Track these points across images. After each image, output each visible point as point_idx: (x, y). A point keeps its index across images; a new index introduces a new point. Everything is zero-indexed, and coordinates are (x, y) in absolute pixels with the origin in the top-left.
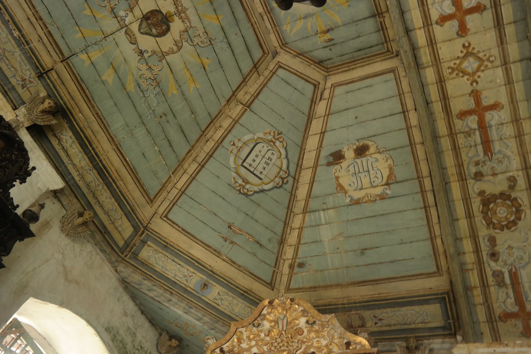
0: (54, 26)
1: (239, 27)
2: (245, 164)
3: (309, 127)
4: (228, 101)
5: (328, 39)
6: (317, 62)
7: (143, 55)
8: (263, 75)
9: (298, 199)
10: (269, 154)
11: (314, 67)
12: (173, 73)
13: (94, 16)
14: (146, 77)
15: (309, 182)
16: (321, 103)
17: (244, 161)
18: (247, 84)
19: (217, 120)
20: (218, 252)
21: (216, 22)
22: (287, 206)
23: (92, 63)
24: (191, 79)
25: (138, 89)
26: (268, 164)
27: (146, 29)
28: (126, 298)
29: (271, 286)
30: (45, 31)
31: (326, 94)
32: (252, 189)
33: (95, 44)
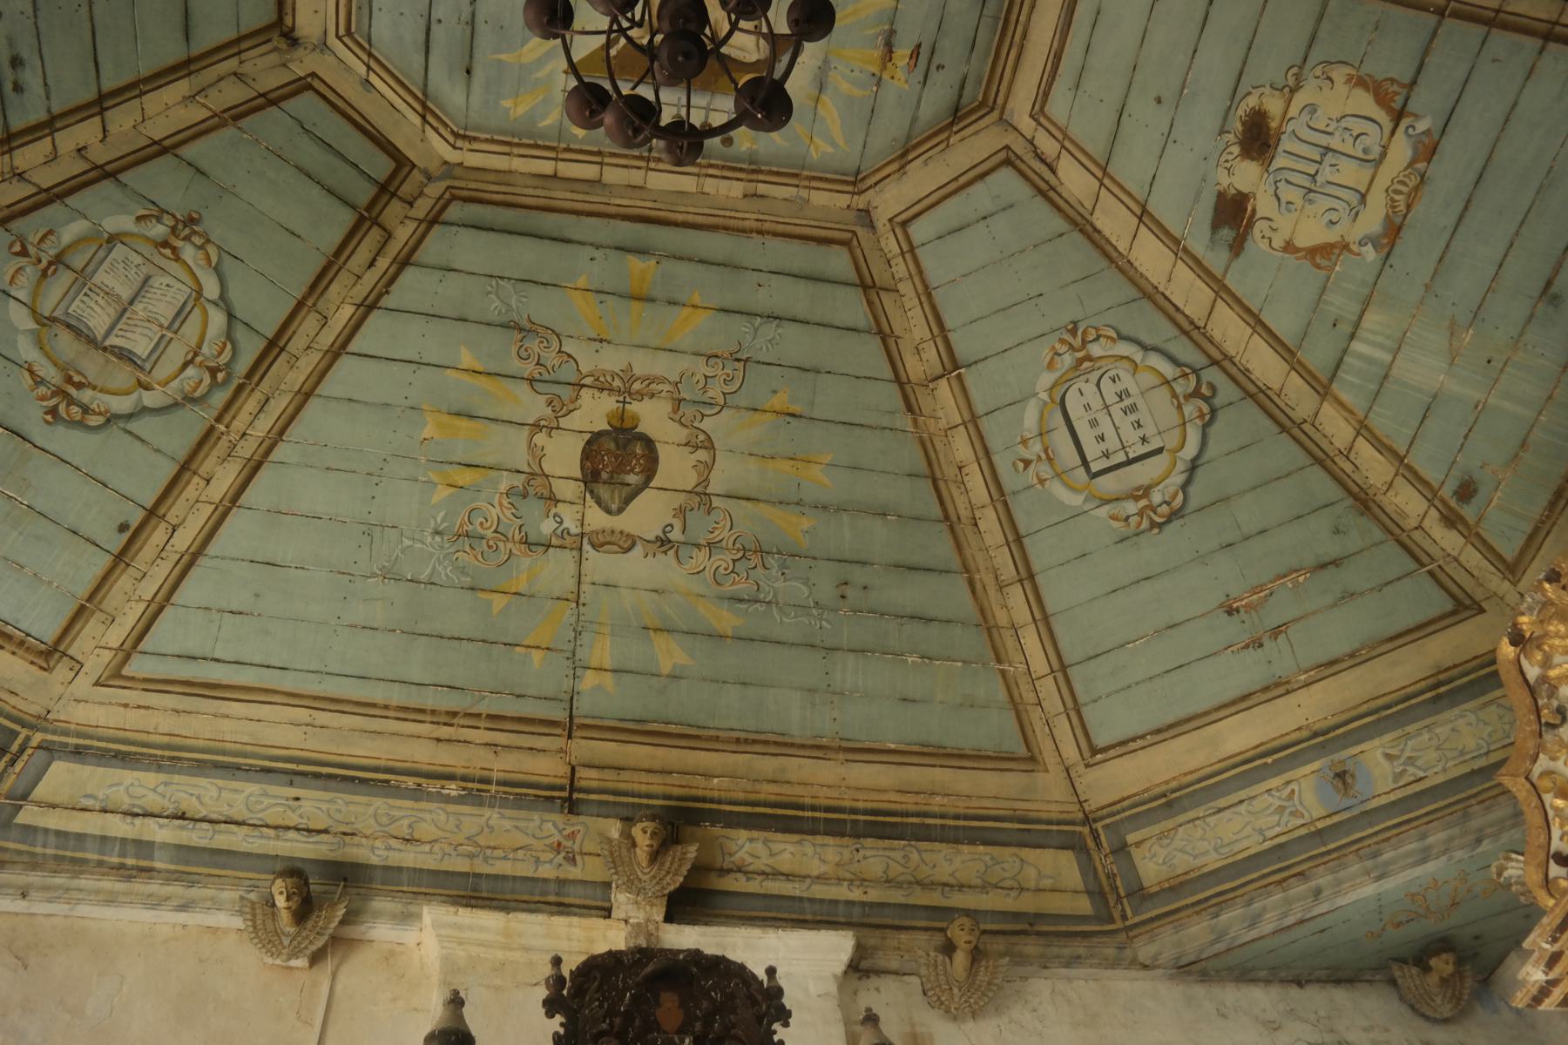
0: (484, 697)
2: (1095, 467)
3: (1103, 242)
4: (910, 409)
5: (911, 57)
7: (670, 541)
8: (900, 280)
9: (1276, 387)
10: (1109, 388)
11: (959, 136)
13: (515, 594)
14: (726, 569)
15: (1249, 331)
16: (1060, 173)
17: (1085, 463)
18: (897, 333)
20: (1277, 685)
21: (702, 318)
22: (1276, 429)
24: (800, 465)
25: (744, 606)
26: (1133, 408)
27: (617, 496)
28: (1231, 994)
29: (1467, 608)
30: (482, 724)
31: (1048, 146)
32: (1172, 489)
33: (577, 633)
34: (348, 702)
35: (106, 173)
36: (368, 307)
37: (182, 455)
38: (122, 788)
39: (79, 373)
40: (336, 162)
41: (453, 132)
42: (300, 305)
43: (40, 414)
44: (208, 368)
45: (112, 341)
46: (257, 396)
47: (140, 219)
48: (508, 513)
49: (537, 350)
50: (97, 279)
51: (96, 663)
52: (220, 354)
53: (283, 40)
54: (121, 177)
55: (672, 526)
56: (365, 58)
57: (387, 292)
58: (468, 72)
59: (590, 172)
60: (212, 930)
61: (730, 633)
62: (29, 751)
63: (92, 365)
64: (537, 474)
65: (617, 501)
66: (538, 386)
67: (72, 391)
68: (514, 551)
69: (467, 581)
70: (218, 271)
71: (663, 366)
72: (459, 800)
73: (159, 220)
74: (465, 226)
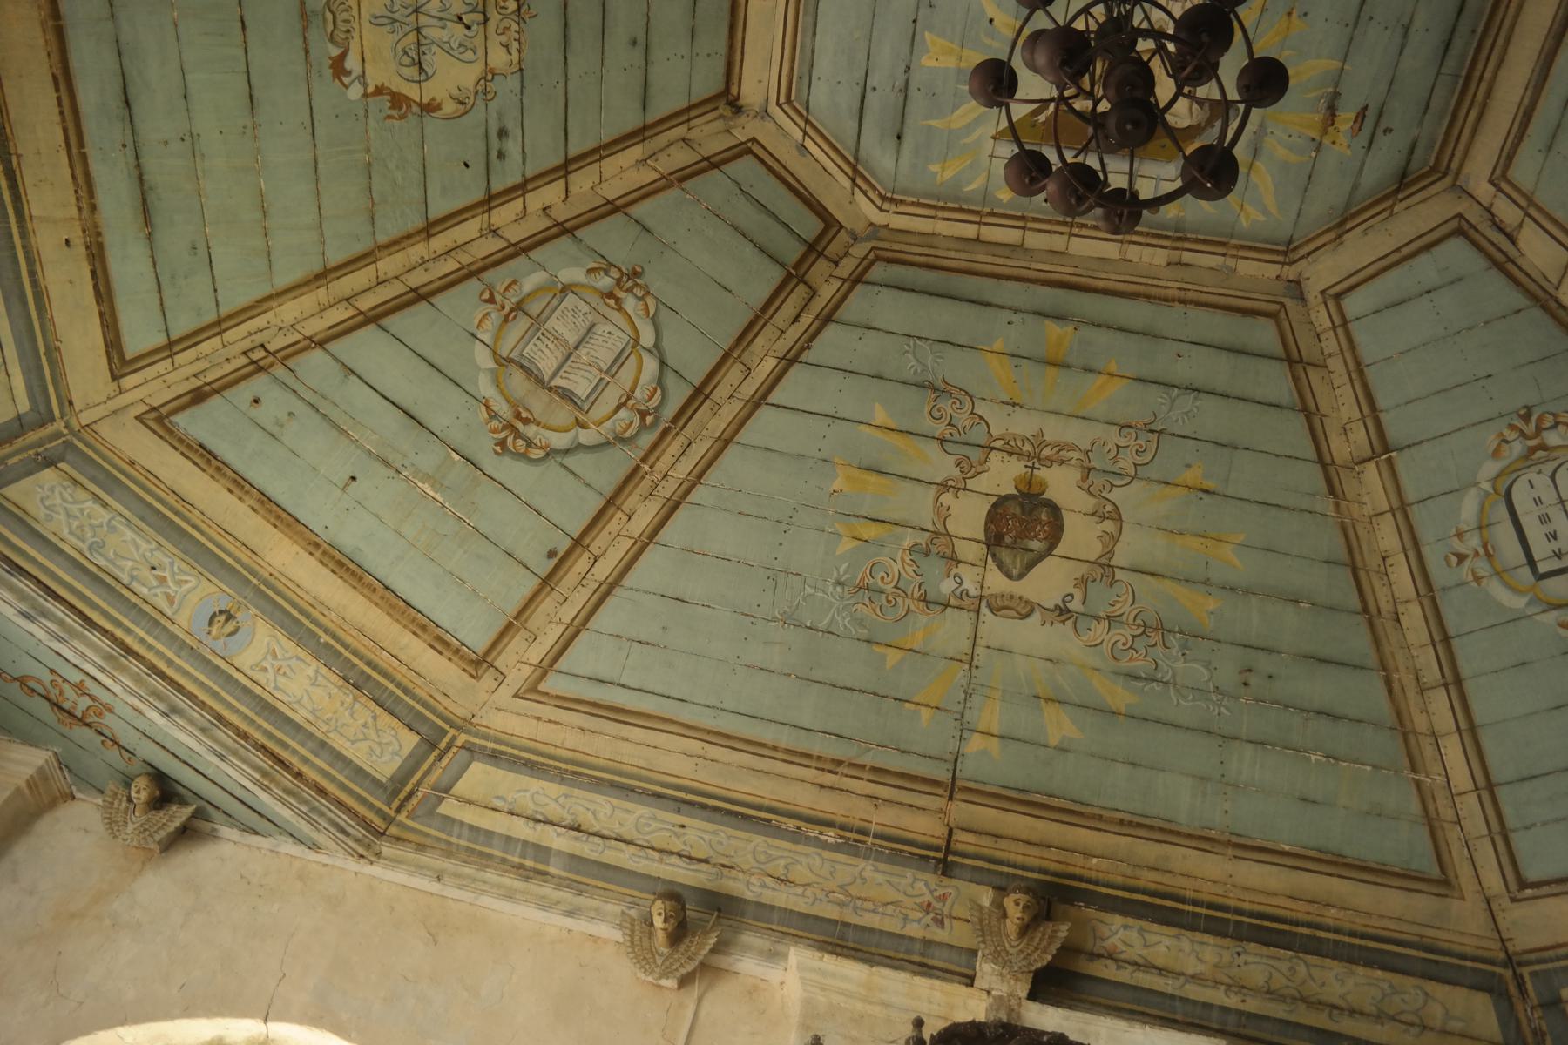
0: (870, 749)
1: (1166, 338)
2: (1543, 568)
4: (1332, 491)
5: (1355, 122)
6: (1397, 185)
7: (1069, 611)
12: (1162, 576)
13: (910, 650)
14: (1124, 644)
16: (1521, 244)
17: (1531, 562)
18: (1323, 411)
19: (1361, 553)
21: (1117, 386)
23: (1002, 737)
24: (1210, 543)
30: (865, 776)
31: (1508, 213)
33: (968, 695)
34: (740, 739)
35: (564, 230)
36: (790, 360)
37: (609, 490)
38: (528, 794)
39: (528, 410)
40: (769, 221)
41: (880, 195)
42: (726, 356)
43: (491, 445)
44: (638, 411)
45: (557, 382)
46: (681, 440)
47: (590, 271)
48: (909, 570)
49: (949, 410)
50: (550, 324)
51: (518, 676)
52: (650, 398)
53: (728, 108)
54: (578, 233)
55: (1072, 596)
56: (802, 124)
57: (808, 347)
58: (899, 137)
59: (1012, 236)
60: (594, 939)
61: (1123, 710)
62: (454, 750)
63: (538, 403)
64: (941, 534)
65: (1018, 566)
66: (949, 447)
67: (519, 425)
68: (912, 607)
69: (864, 633)
70: (654, 321)
71: (1075, 433)
72: (836, 848)
73: (606, 272)
74: (887, 286)
